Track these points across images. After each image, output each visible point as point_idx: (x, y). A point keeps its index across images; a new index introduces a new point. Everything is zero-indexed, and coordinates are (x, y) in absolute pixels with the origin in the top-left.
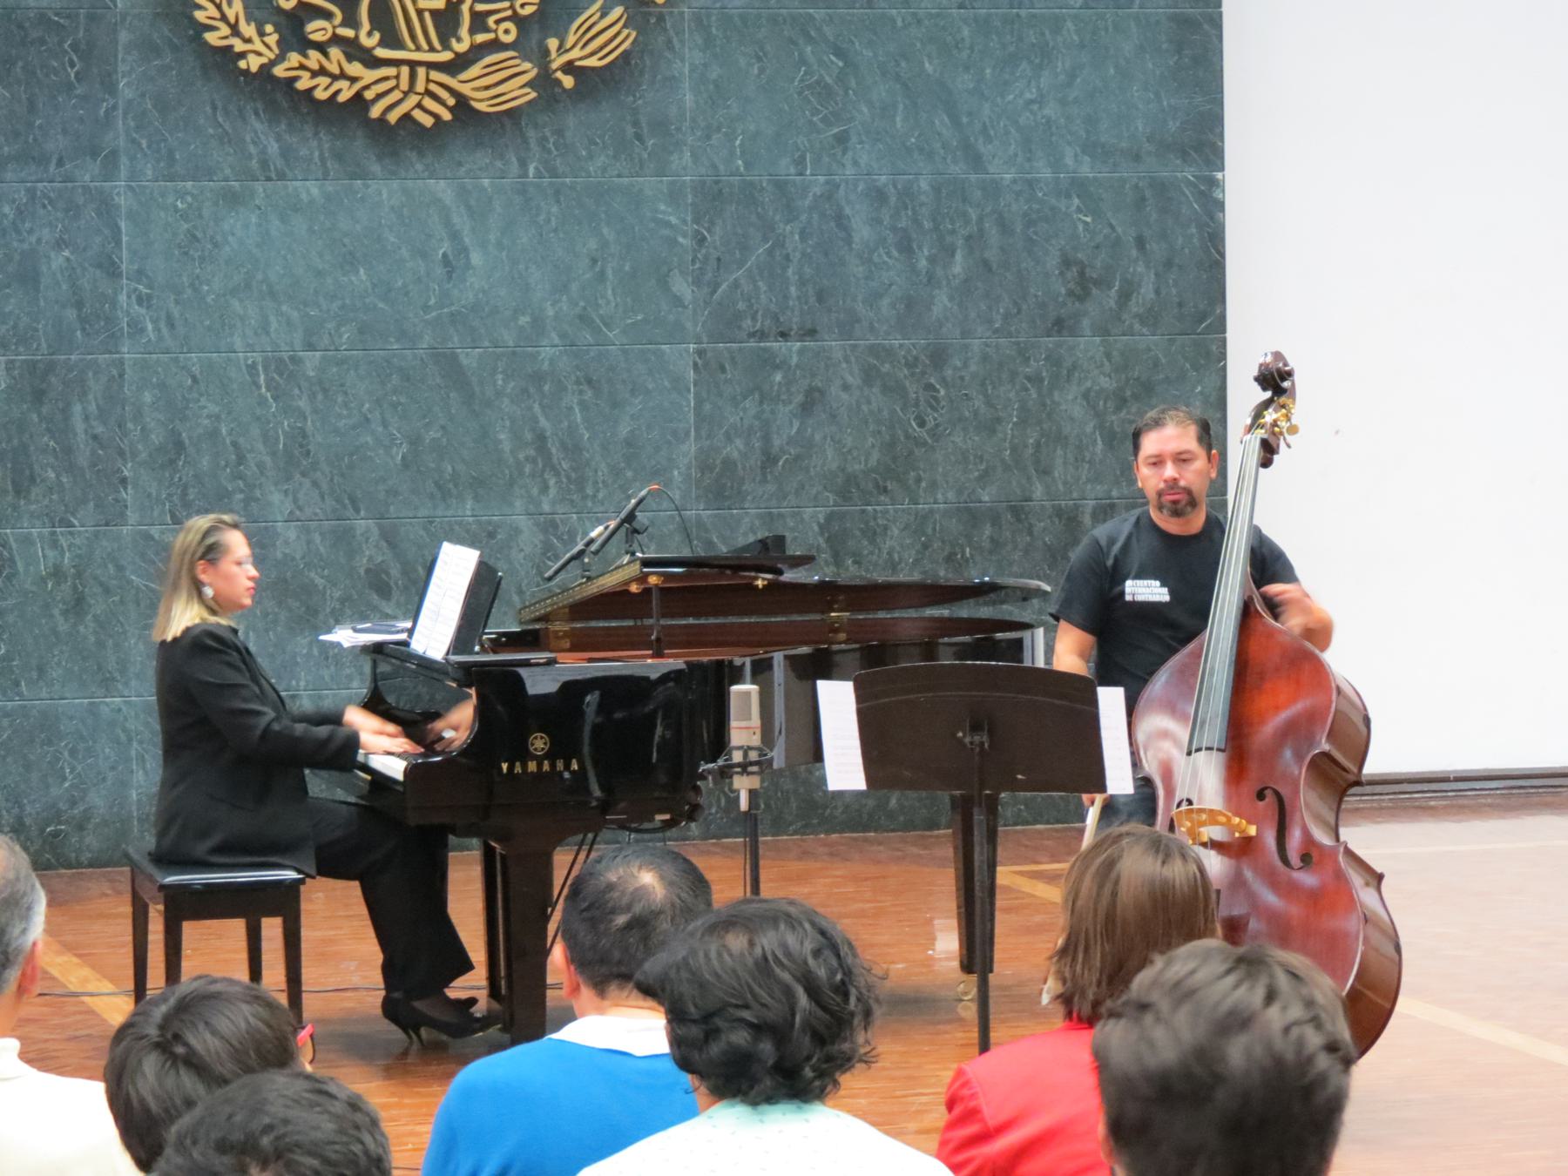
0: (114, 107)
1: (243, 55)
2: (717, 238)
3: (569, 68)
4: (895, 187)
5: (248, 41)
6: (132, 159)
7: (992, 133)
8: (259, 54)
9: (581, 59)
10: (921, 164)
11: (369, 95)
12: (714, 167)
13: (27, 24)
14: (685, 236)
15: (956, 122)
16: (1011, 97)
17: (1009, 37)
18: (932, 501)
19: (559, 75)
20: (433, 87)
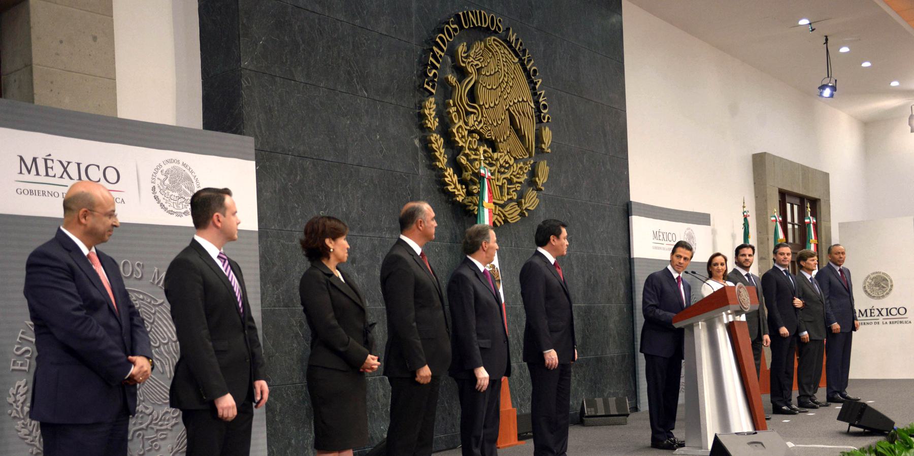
1: (457, 196)
3: (526, 209)
5: (459, 190)
8: (462, 196)
13: (397, 178)
19: (525, 211)
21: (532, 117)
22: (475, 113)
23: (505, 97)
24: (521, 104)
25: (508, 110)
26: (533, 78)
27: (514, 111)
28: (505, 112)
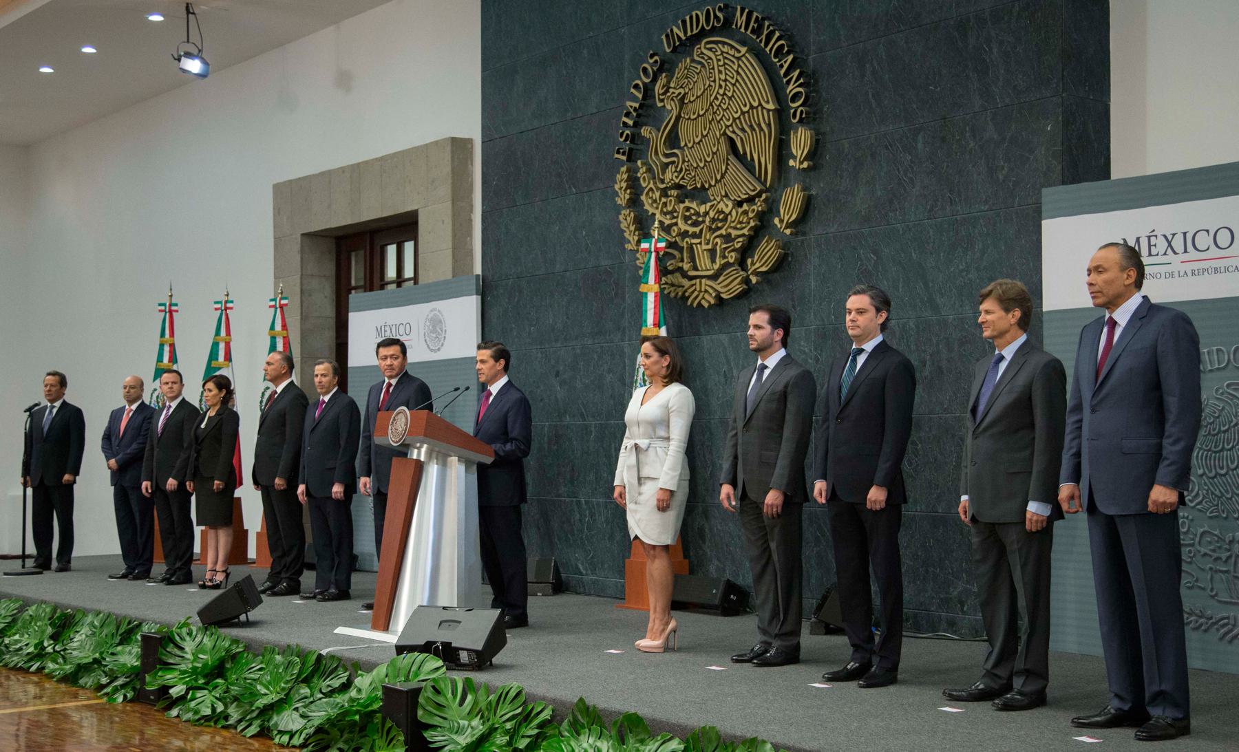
0: (624, 308)
2: (824, 359)
3: (755, 273)
4: (899, 327)
6: (630, 331)
7: (943, 291)
9: (762, 266)
10: (910, 313)
11: (687, 294)
12: (823, 321)
14: (811, 359)
15: (926, 285)
16: (952, 269)
17: (952, 233)
18: (914, 510)
20: (708, 288)
21: (769, 125)
22: (673, 163)
23: (718, 118)
24: (746, 115)
25: (725, 134)
26: (776, 60)
27: (734, 132)
28: (718, 140)
